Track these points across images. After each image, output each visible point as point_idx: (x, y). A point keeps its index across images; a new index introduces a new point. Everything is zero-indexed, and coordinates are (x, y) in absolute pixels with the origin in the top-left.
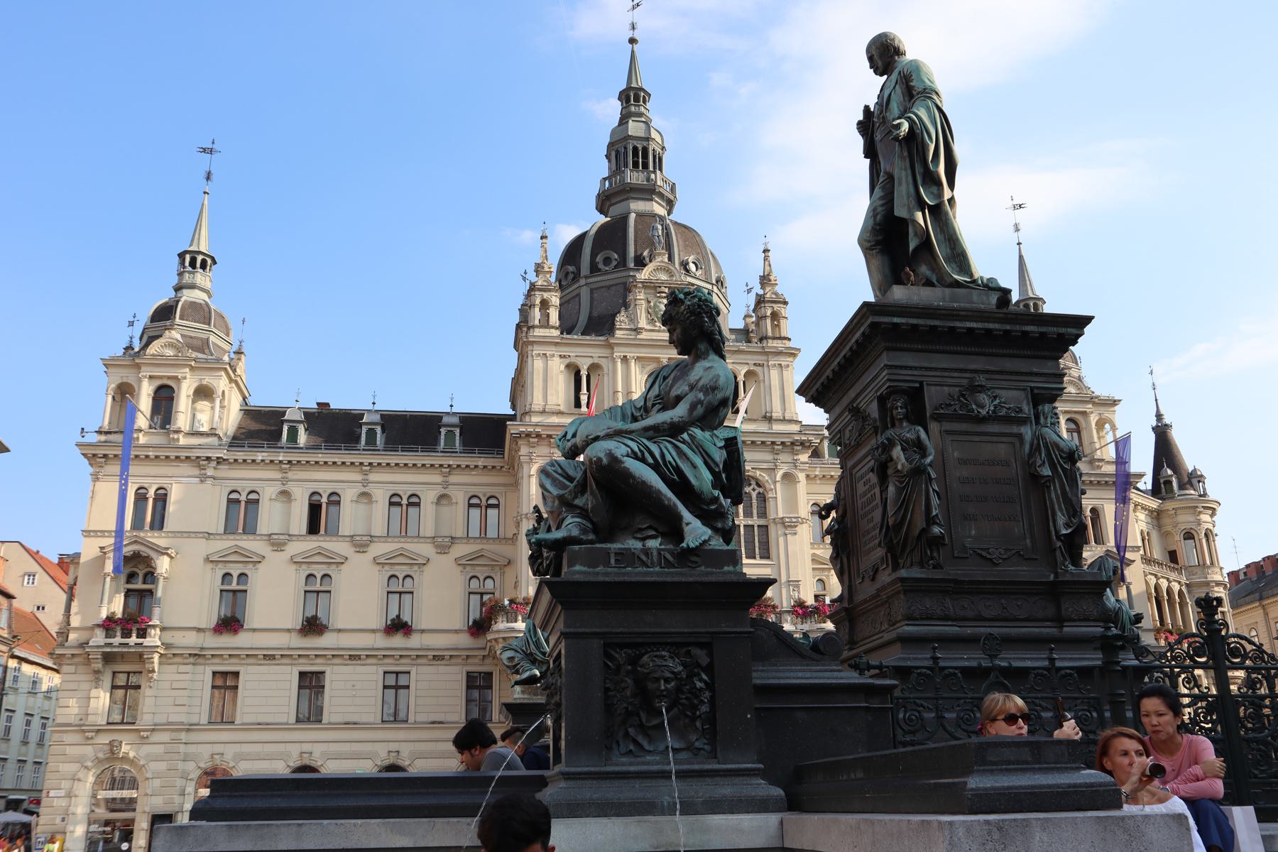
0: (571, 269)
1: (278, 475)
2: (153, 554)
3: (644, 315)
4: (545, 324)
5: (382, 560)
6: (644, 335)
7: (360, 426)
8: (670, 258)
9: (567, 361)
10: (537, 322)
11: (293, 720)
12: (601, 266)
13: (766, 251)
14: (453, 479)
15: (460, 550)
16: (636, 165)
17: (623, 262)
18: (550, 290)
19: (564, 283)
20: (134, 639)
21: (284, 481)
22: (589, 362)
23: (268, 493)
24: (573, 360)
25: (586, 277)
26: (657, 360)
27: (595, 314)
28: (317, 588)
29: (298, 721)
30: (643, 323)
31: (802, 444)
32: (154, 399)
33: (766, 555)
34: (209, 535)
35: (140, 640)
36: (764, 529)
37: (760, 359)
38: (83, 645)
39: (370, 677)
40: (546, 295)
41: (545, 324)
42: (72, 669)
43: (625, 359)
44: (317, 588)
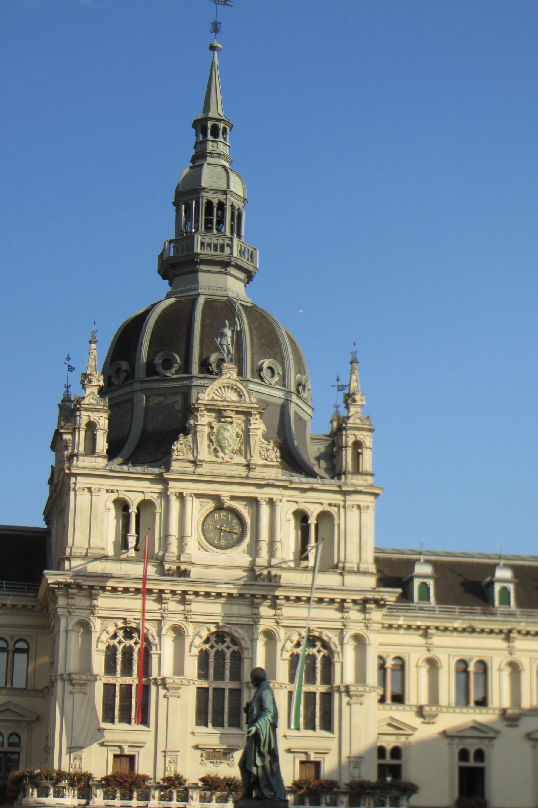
0: (124, 365)
3: (206, 442)
4: (91, 450)
6: (203, 469)
8: (240, 373)
9: (114, 496)
10: (82, 449)
12: (159, 369)
16: (209, 222)
17: (186, 367)
18: (98, 410)
19: (116, 381)
22: (140, 497)
24: (122, 495)
25: (142, 382)
26: (217, 498)
27: (150, 428)
30: (204, 453)
31: (376, 602)
33: (327, 725)
36: (327, 697)
37: (338, 498)
40: (94, 416)
41: (91, 450)
43: (181, 497)
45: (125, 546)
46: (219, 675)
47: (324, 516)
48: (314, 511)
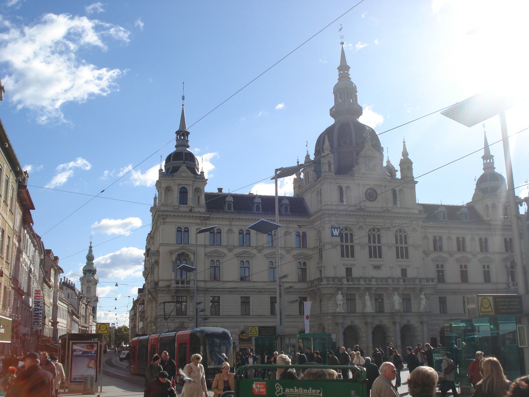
1: (228, 223)
2: (189, 253)
4: (330, 171)
5: (268, 256)
7: (253, 204)
11: (240, 314)
13: (404, 142)
14: (290, 225)
15: (295, 252)
20: (185, 285)
21: (231, 225)
23: (224, 230)
24: (340, 184)
28: (245, 265)
29: (242, 315)
32: (180, 192)
34: (205, 246)
35: (188, 285)
38: (169, 286)
39: (266, 299)
42: (162, 295)
44: (245, 265)
45: (342, 201)
46: (374, 242)
47: (401, 190)
48: (397, 189)
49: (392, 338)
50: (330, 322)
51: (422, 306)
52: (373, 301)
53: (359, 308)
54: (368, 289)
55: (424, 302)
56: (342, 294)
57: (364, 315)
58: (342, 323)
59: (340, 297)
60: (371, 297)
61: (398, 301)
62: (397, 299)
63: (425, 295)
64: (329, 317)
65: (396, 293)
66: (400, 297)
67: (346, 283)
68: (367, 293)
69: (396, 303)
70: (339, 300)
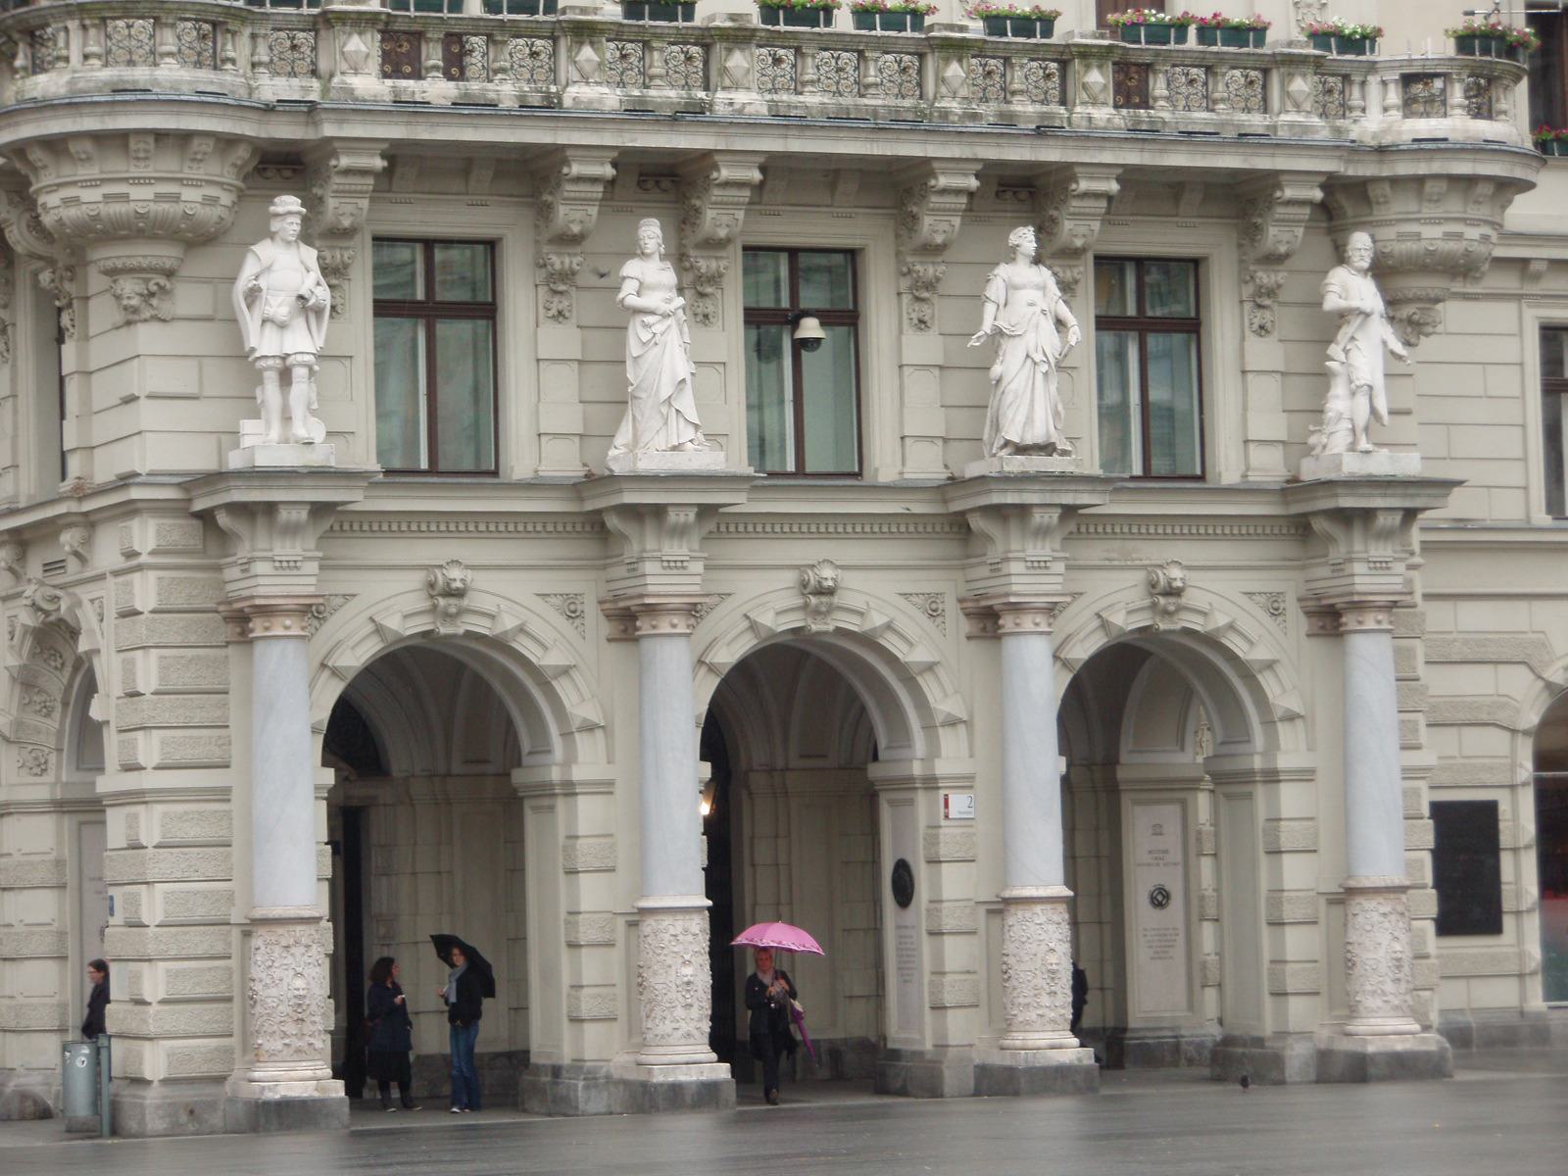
49: (959, 803)
50: (145, 591)
51: (1338, 402)
52: (730, 337)
53: (540, 422)
54: (664, 181)
55: (1366, 354)
56: (315, 231)
57: (601, 517)
58: (312, 612)
59: (282, 266)
60: (696, 286)
61: (1047, 340)
62: (1032, 314)
63: (1382, 270)
64: (145, 534)
65: (1025, 238)
66: (1066, 288)
67: (369, 84)
68: (651, 232)
69: (1010, 365)
70: (278, 305)
